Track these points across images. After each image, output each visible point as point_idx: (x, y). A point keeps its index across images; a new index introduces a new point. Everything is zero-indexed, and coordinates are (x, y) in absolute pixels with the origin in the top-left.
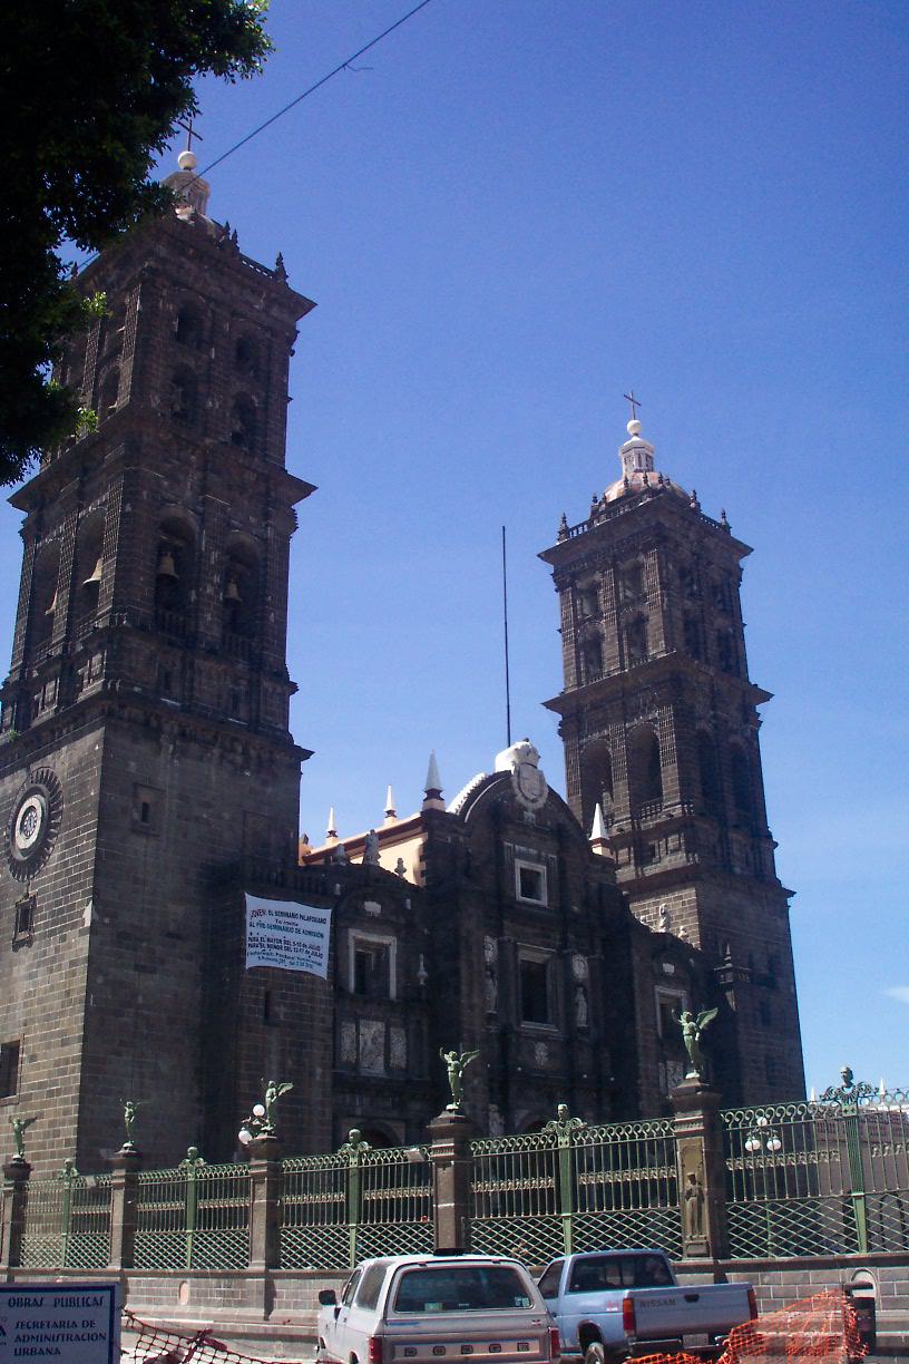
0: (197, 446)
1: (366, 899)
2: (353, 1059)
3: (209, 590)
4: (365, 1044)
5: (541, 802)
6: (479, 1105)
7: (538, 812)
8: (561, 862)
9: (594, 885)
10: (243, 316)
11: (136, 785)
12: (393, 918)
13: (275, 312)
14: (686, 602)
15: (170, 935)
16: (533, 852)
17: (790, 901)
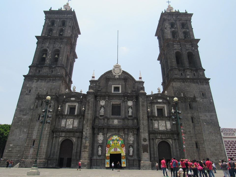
0: (48, 38)
1: (71, 97)
2: (64, 126)
3: (48, 57)
4: (68, 123)
5: (120, 74)
6: (88, 133)
7: (119, 76)
8: (125, 84)
9: (136, 87)
10: (62, 18)
11: (28, 88)
12: (78, 100)
13: (68, 15)
14: (172, 29)
15: (30, 109)
16: (117, 83)
17: (209, 81)
